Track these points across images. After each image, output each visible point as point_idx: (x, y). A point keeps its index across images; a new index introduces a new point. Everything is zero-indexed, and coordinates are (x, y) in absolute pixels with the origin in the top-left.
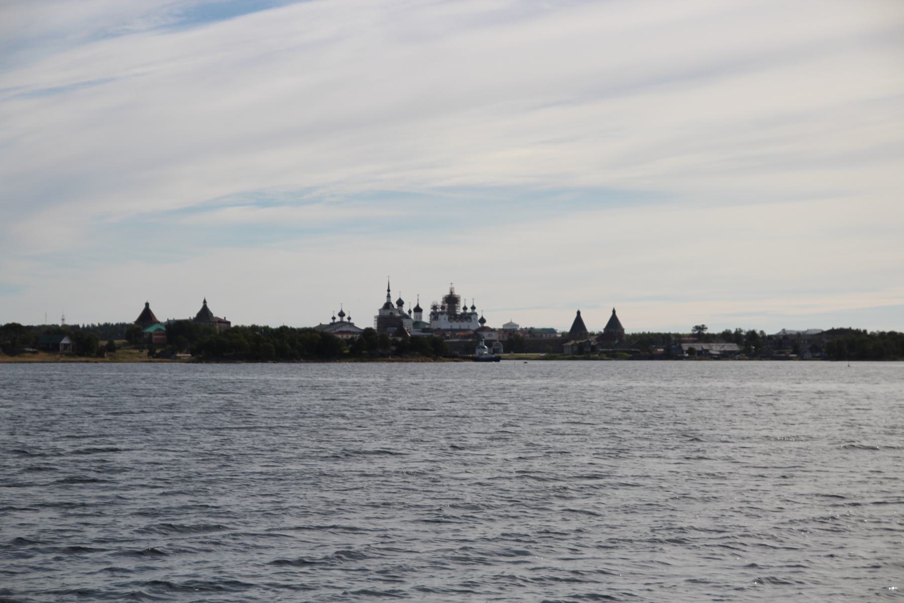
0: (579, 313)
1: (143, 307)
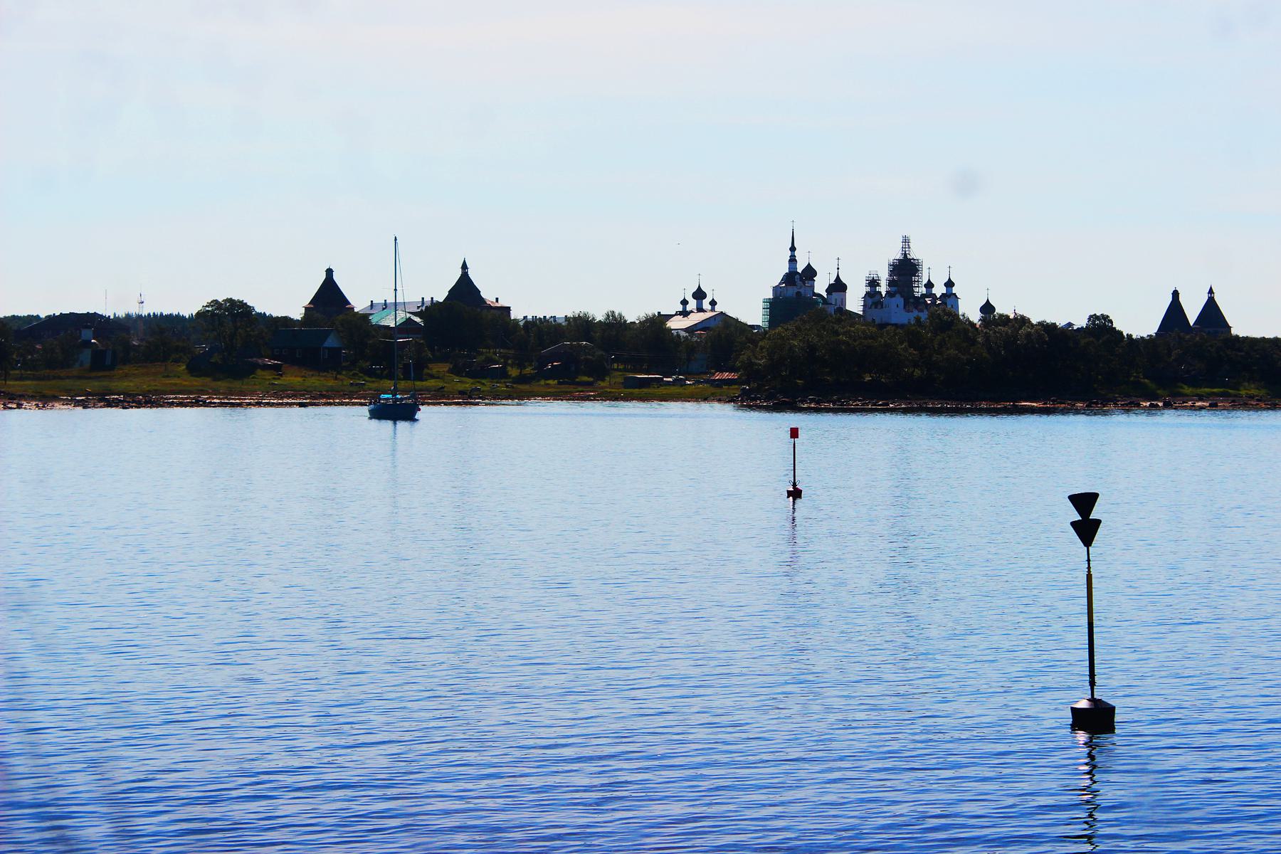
1: (323, 277)
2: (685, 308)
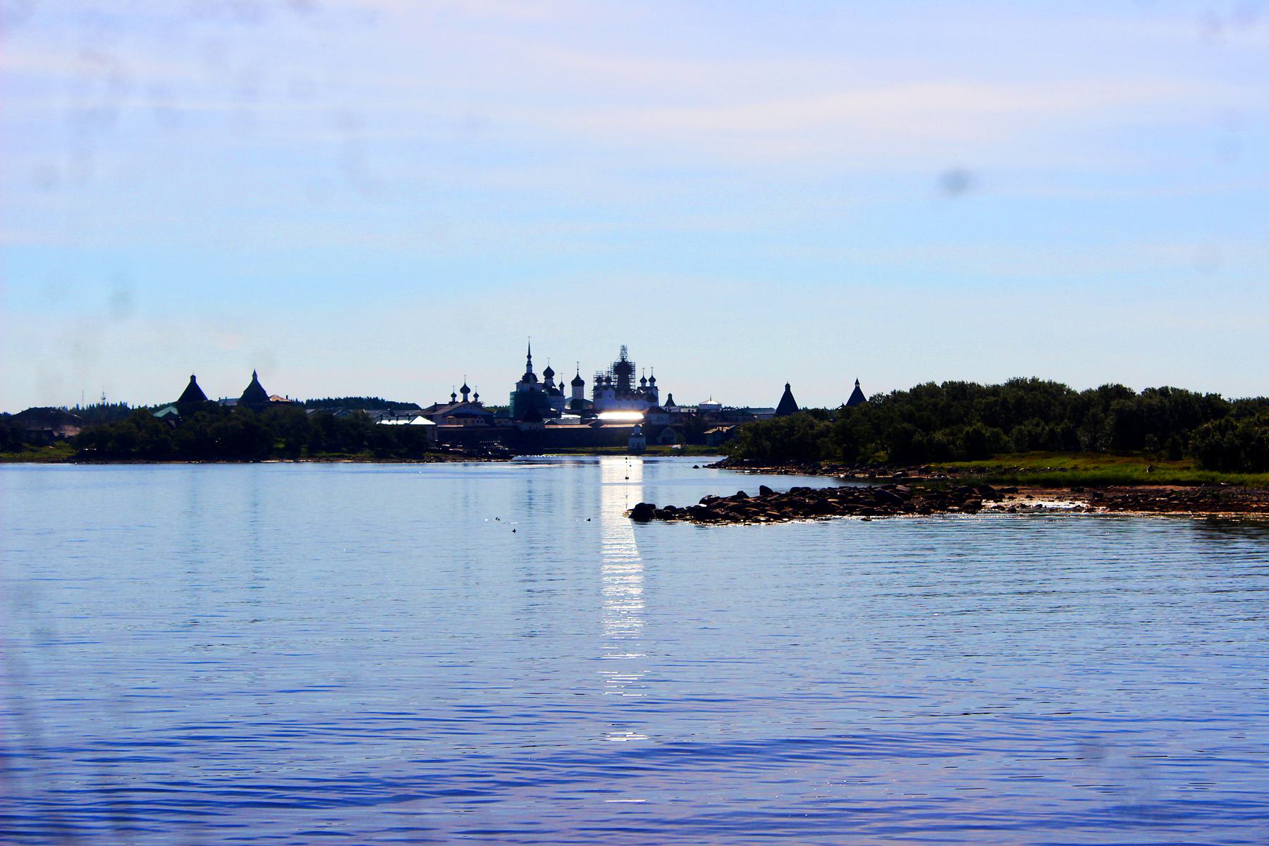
0: (788, 386)
2: (454, 400)
